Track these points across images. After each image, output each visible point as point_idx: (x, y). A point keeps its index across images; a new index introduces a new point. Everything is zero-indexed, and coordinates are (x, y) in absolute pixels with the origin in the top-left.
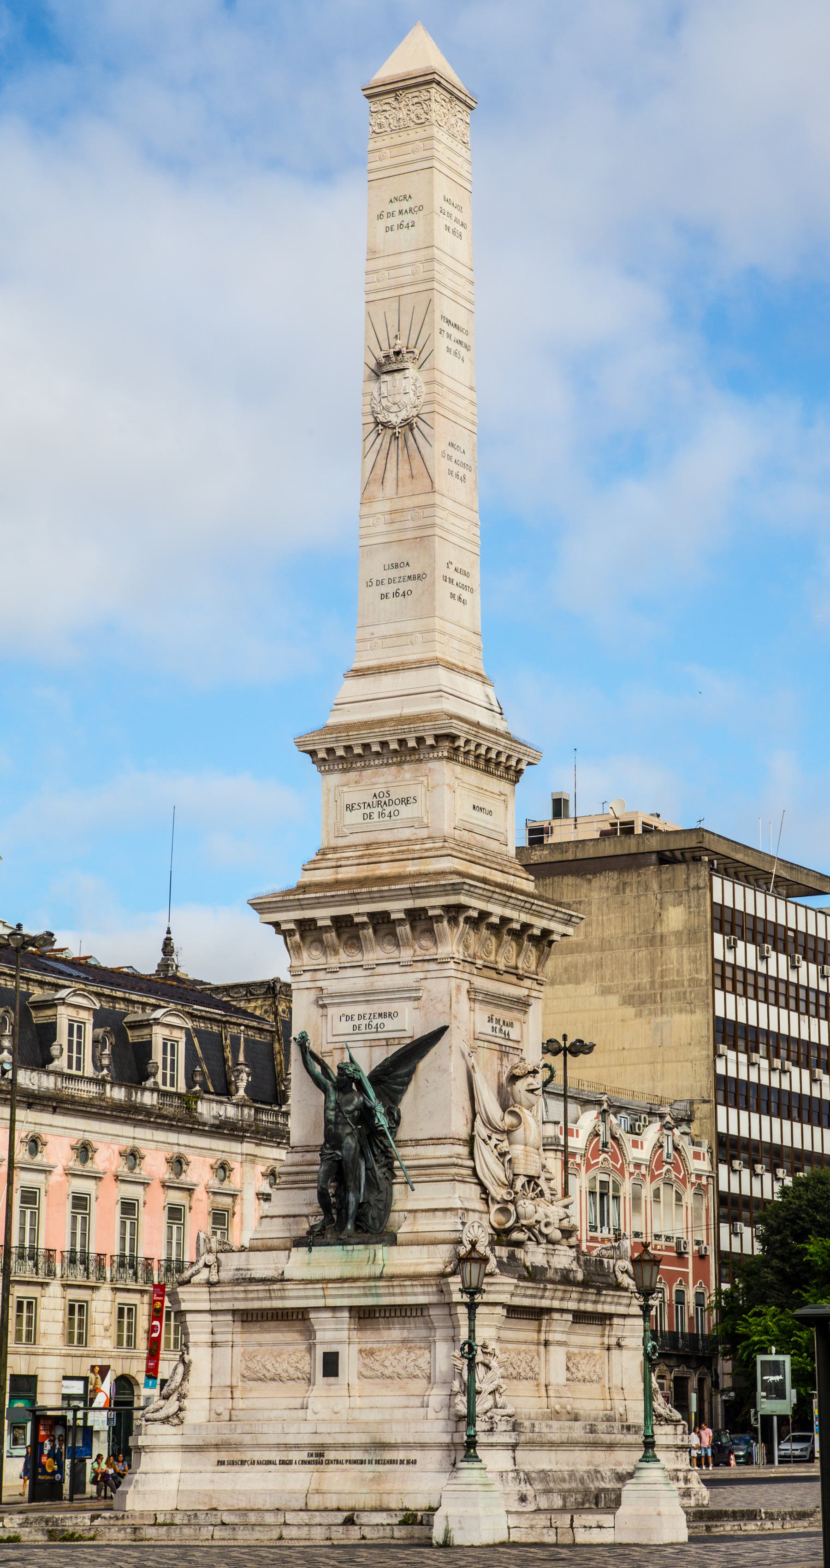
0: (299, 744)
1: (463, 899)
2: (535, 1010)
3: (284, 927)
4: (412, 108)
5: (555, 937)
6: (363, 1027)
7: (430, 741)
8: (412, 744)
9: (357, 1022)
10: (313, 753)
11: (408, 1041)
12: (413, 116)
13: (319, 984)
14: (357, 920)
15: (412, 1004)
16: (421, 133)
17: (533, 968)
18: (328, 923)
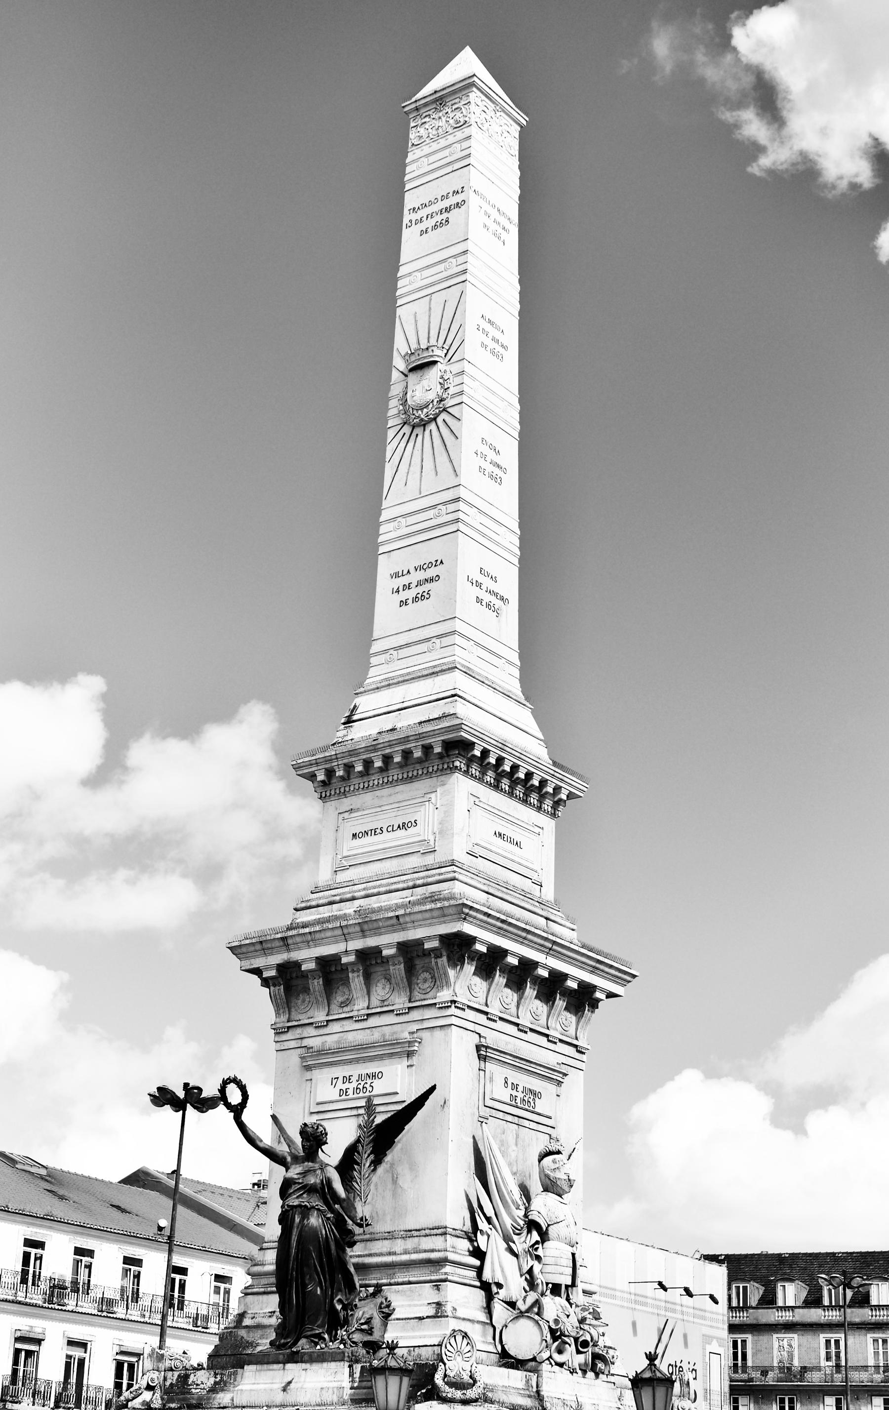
0: (297, 767)
1: (469, 929)
2: (575, 1081)
3: (266, 974)
4: (451, 115)
5: (598, 995)
6: (350, 1092)
7: (438, 750)
8: (418, 754)
9: (344, 1087)
10: (312, 777)
11: (399, 1107)
12: (451, 121)
13: (306, 1042)
14: (344, 960)
15: (405, 1062)
16: (460, 135)
17: (572, 1031)
18: (312, 966)
